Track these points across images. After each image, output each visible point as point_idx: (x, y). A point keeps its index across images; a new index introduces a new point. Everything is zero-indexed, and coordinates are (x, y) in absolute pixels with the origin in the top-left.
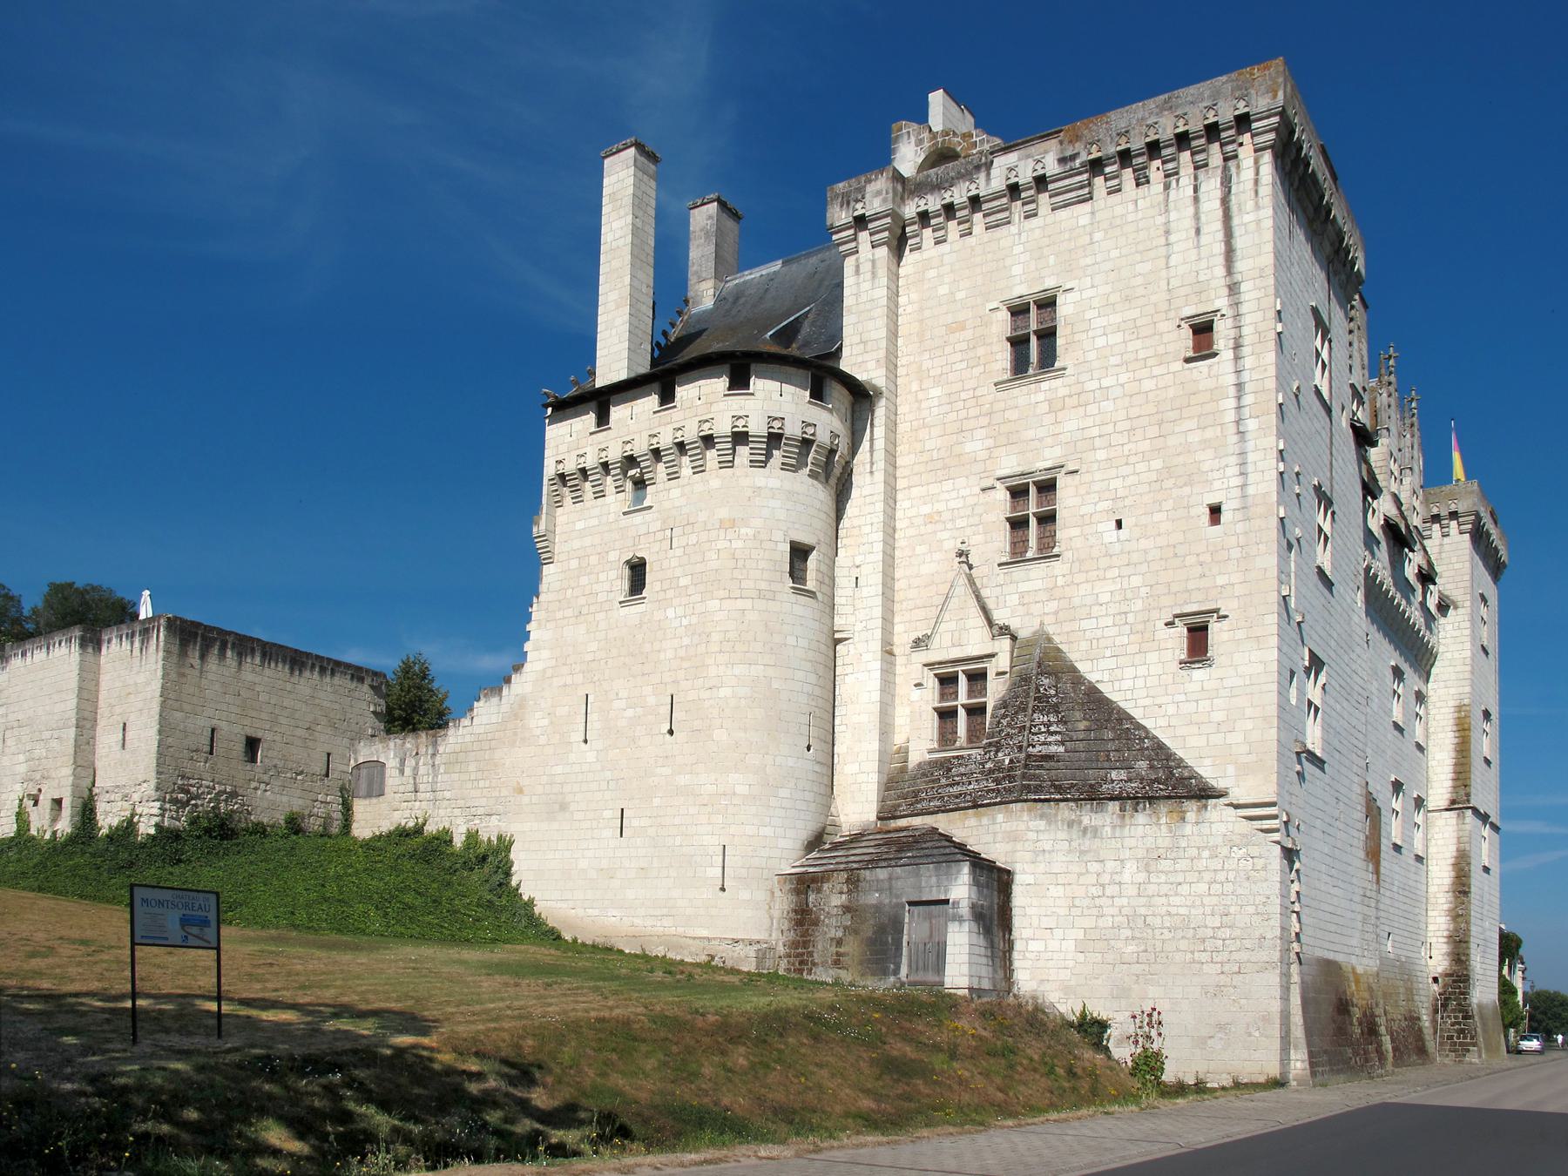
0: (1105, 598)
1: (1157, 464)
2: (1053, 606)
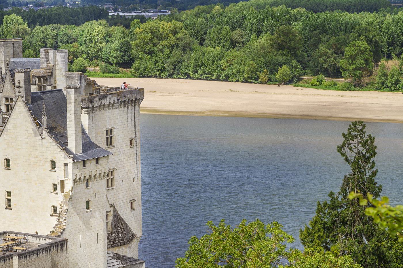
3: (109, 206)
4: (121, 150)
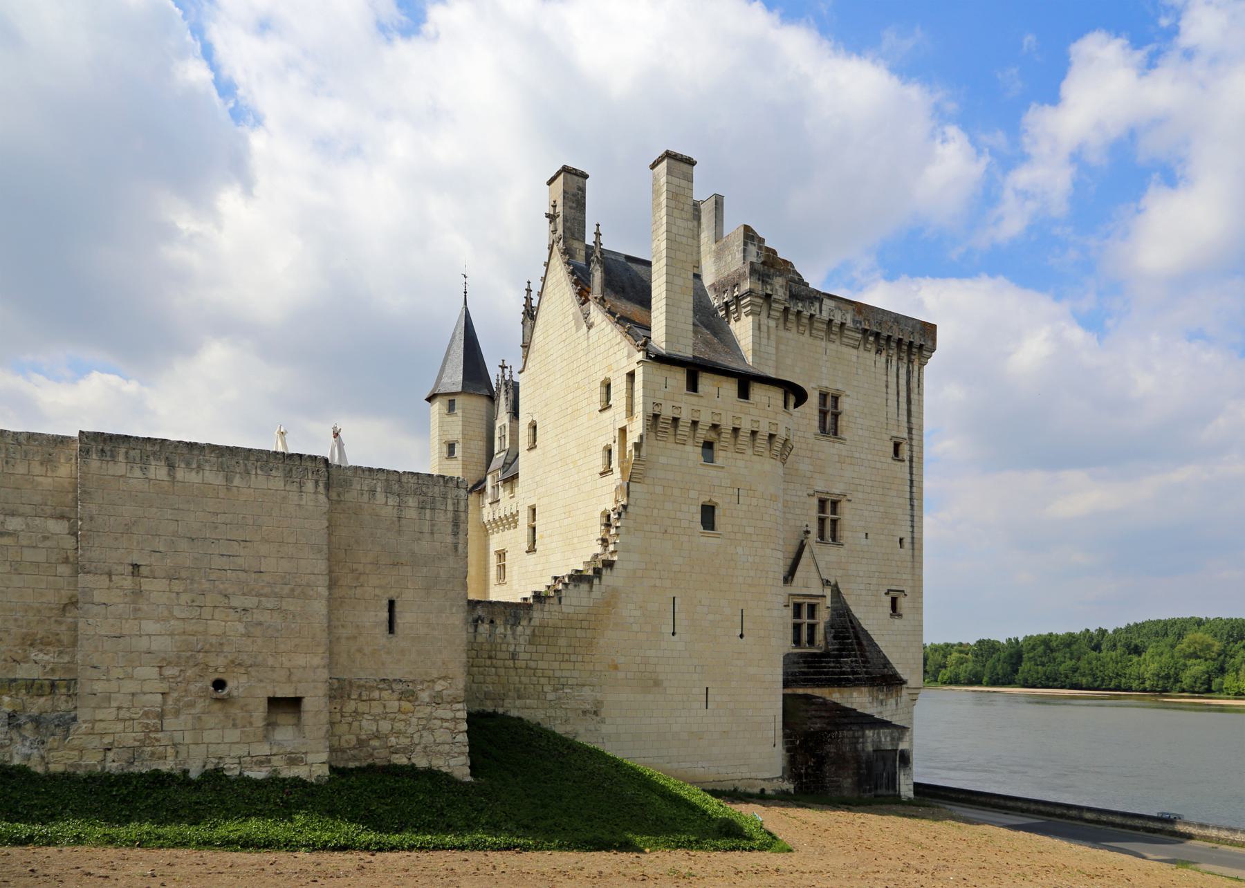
0: (861, 574)
1: (882, 509)
2: (839, 573)
3: (819, 583)
4: (863, 456)
